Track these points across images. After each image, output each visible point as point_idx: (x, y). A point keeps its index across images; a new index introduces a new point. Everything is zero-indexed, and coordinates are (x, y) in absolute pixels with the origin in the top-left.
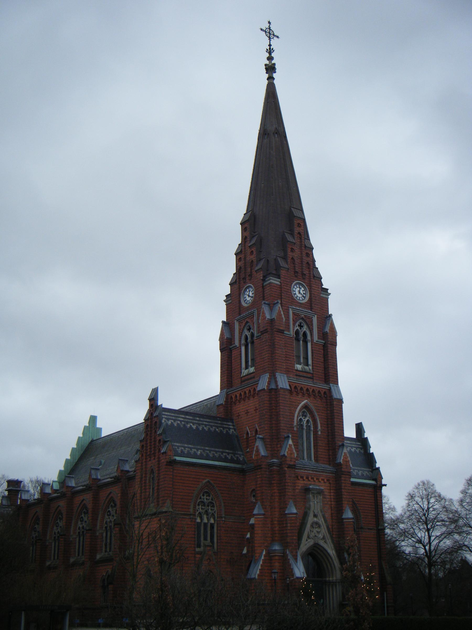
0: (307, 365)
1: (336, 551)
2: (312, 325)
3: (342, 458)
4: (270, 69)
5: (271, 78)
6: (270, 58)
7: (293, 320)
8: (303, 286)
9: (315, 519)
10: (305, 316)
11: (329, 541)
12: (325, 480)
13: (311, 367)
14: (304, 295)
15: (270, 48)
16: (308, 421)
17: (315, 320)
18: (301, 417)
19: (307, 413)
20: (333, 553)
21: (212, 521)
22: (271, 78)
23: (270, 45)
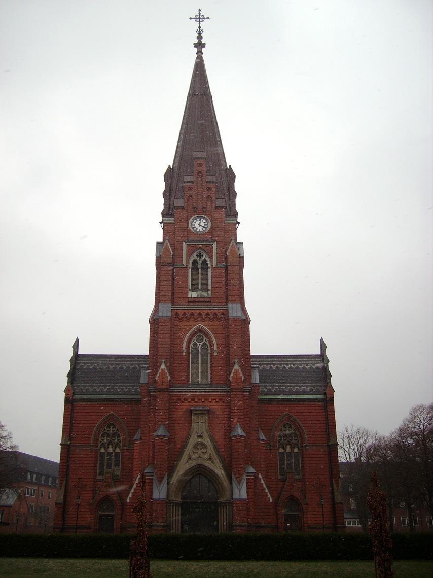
0: (207, 290)
1: (225, 470)
2: (212, 251)
3: (232, 375)
4: (200, 45)
5: (200, 53)
6: (200, 37)
7: (188, 251)
8: (204, 218)
9: (200, 440)
10: (203, 245)
11: (217, 461)
12: (217, 400)
13: (210, 292)
14: (206, 226)
15: (200, 30)
16: (204, 344)
17: (215, 246)
18: (195, 341)
19: (203, 337)
20: (221, 473)
21: (118, 450)
22: (200, 53)
23: (200, 27)
